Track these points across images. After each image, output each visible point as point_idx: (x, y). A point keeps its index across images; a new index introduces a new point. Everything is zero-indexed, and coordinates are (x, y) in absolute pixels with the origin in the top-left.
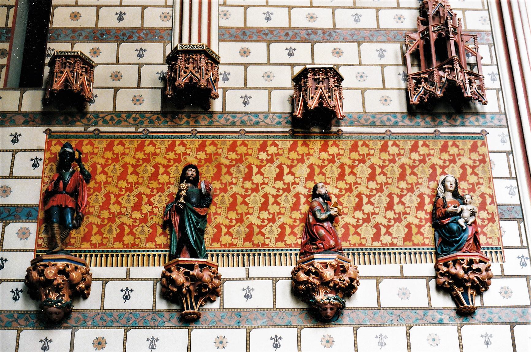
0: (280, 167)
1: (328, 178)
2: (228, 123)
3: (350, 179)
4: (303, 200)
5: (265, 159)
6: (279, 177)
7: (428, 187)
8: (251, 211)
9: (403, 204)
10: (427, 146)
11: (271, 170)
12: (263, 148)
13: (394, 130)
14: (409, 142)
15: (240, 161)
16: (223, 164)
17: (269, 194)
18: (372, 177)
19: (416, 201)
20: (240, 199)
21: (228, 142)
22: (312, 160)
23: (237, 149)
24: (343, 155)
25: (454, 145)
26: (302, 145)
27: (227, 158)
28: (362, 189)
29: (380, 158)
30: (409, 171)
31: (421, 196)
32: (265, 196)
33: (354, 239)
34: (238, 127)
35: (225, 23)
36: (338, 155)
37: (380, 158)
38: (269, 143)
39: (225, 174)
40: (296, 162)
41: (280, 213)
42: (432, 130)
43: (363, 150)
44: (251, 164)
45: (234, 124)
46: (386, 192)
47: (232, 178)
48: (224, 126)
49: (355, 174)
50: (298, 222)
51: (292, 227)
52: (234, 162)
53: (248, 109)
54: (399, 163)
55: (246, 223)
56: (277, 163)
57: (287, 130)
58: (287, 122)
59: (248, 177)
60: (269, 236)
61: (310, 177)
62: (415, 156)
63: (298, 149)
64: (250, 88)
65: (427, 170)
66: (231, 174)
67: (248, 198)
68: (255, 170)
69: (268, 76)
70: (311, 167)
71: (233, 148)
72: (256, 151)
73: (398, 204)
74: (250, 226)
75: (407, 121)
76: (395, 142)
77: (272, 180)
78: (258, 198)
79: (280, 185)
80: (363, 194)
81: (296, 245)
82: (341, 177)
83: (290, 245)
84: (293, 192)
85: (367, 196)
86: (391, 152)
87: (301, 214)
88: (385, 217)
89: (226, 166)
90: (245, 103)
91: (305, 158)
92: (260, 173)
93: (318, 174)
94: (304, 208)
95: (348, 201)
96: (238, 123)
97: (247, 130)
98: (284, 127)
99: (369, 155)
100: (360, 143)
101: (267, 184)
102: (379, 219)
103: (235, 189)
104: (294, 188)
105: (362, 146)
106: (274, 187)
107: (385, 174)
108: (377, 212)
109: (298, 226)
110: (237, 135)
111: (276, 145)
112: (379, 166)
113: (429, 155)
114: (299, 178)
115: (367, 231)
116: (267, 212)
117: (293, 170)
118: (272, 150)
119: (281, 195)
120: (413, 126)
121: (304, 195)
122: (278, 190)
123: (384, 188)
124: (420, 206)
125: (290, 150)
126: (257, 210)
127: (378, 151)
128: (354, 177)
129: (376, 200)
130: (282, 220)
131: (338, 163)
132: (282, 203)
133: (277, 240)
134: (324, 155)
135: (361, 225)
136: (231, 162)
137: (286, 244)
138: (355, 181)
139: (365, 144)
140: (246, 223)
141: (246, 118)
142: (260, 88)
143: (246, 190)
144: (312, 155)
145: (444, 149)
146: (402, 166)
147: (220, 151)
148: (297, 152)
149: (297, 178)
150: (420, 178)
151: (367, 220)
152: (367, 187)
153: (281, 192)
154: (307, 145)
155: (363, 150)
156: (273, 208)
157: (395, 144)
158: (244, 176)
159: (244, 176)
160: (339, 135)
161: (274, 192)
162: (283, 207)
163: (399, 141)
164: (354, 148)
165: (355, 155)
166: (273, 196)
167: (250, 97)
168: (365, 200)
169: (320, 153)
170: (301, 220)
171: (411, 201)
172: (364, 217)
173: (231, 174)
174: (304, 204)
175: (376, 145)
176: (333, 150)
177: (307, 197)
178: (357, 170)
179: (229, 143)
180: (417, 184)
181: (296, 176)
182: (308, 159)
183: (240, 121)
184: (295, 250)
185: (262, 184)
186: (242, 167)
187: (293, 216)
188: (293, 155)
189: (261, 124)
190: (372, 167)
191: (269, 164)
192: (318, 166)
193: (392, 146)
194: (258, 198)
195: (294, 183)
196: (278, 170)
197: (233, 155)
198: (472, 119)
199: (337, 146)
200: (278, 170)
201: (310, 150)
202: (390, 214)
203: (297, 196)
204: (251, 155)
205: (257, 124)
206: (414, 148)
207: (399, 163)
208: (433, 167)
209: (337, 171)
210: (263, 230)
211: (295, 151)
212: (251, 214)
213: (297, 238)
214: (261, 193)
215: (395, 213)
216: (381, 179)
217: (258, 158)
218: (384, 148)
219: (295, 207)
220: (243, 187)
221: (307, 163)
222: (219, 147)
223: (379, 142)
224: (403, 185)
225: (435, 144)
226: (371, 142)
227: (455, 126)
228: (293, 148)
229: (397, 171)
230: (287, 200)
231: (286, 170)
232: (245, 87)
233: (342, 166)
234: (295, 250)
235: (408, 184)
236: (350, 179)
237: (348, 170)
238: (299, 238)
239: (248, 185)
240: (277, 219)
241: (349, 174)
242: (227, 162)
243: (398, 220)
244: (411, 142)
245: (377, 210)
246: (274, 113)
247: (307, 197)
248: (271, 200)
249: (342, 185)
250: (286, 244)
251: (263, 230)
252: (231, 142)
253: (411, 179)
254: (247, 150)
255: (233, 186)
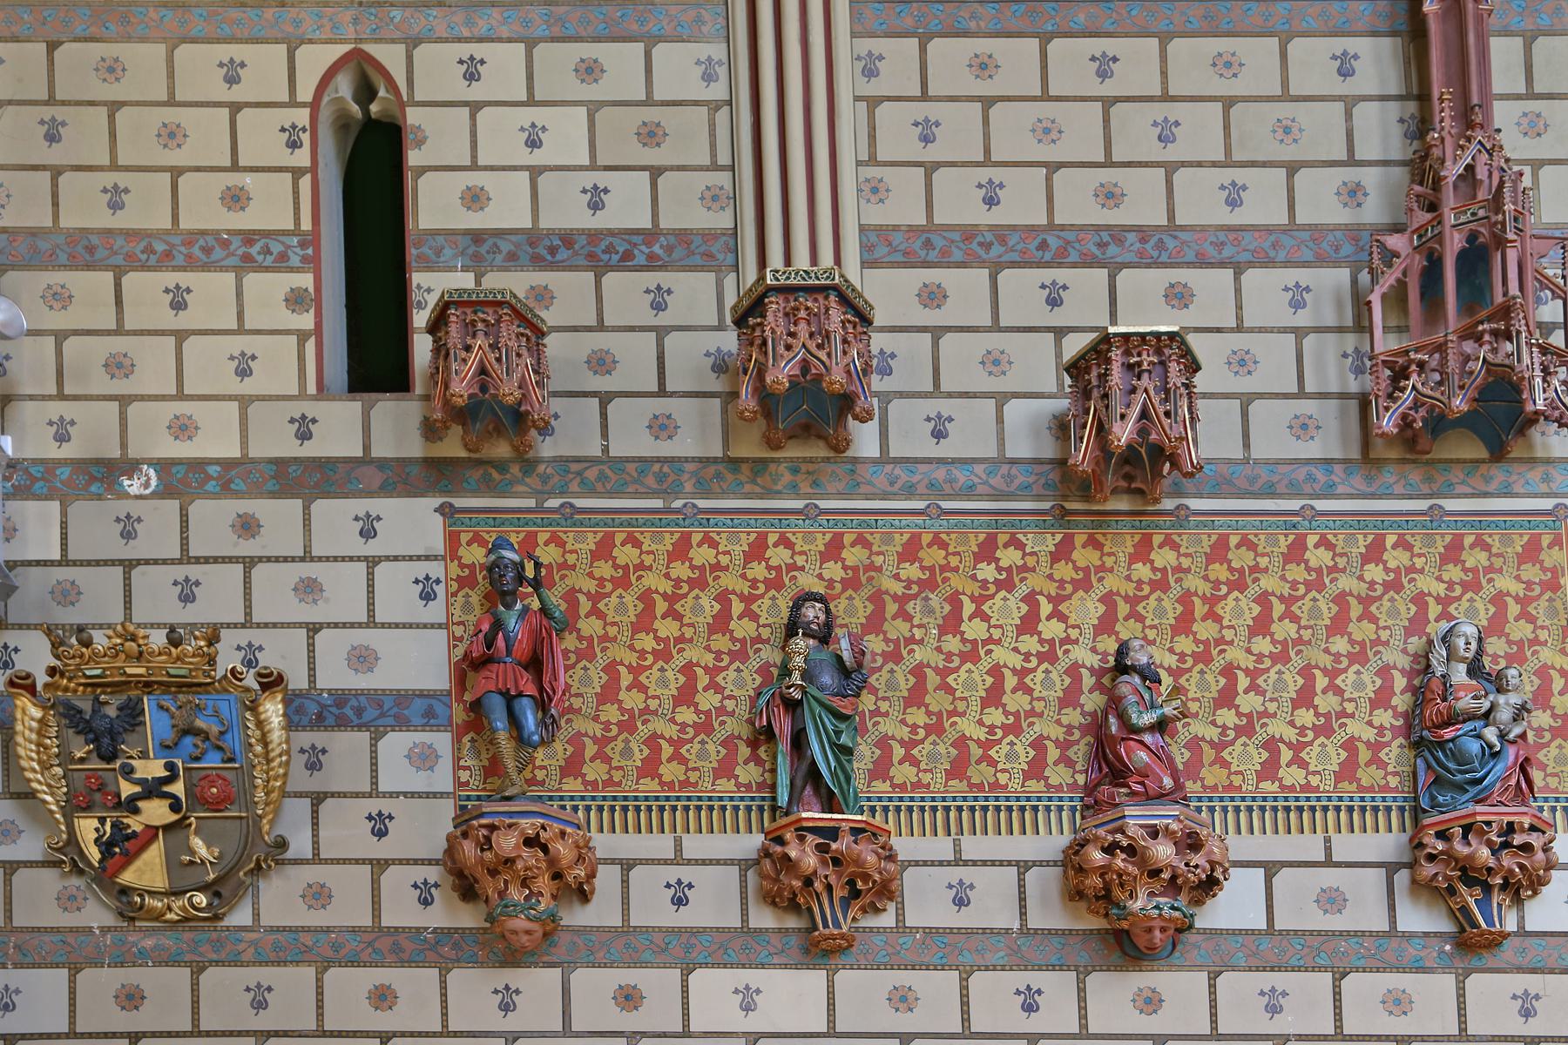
0: (1030, 599)
1: (1152, 627)
2: (897, 486)
3: (1205, 630)
4: (1088, 681)
5: (991, 580)
6: (1029, 624)
7: (1405, 651)
8: (961, 706)
9: (1339, 692)
10: (1408, 547)
11: (1008, 609)
12: (986, 552)
13: (1321, 505)
14: (1360, 537)
15: (929, 584)
16: (887, 592)
17: (1005, 666)
18: (1261, 626)
19: (1371, 683)
20: (932, 679)
21: (897, 536)
22: (1111, 583)
23: (921, 554)
24: (1188, 570)
25: (1480, 544)
26: (1084, 546)
27: (897, 577)
28: (1235, 654)
29: (1283, 578)
30: (1356, 610)
31: (1385, 672)
32: (996, 671)
33: (1212, 775)
34: (921, 497)
35: (877, 215)
36: (1178, 569)
37: (1283, 578)
38: (1002, 539)
39: (894, 618)
40: (1069, 588)
41: (1032, 713)
42: (1422, 505)
43: (1241, 558)
44: (957, 593)
45: (909, 492)
46: (1297, 662)
47: (913, 626)
48: (885, 496)
49: (1218, 619)
50: (1077, 734)
51: (1064, 746)
52: (915, 588)
53: (945, 450)
54: (1332, 589)
55: (951, 735)
56: (1022, 590)
57: (1047, 505)
58: (1046, 485)
59: (952, 624)
60: (1008, 766)
61: (1106, 625)
62: (1374, 572)
63: (1075, 555)
64: (950, 395)
65: (1403, 609)
66: (908, 618)
67: (954, 676)
68: (968, 607)
69: (996, 362)
70: (1108, 599)
71: (910, 553)
72: (969, 560)
73: (1324, 691)
74: (961, 742)
75: (1358, 482)
76: (1323, 536)
77: (1011, 632)
78: (976, 676)
79: (1030, 643)
80: (1239, 668)
81: (1074, 786)
82: (1184, 624)
83: (1059, 788)
84: (1064, 663)
85: (1247, 671)
86: (1313, 564)
87: (1083, 714)
88: (1292, 723)
89: (895, 598)
90: (939, 435)
91: (1094, 579)
92: (979, 614)
93: (1126, 619)
94: (1092, 701)
95: (1202, 685)
96: (921, 489)
97: (945, 505)
98: (1039, 498)
99: (1255, 569)
100: (1234, 540)
101: (998, 642)
102: (1278, 728)
103: (920, 654)
104: (1067, 652)
105: (1238, 546)
106: (1016, 650)
107: (1295, 619)
108: (1271, 711)
109: (1077, 742)
110: (919, 520)
111: (1020, 546)
112: (1281, 598)
113: (1411, 569)
114: (1078, 627)
115: (1246, 757)
116: (1001, 710)
117: (1062, 608)
118: (1009, 557)
119: (1034, 670)
120: (1373, 496)
121: (1092, 670)
122: (1027, 657)
123: (1292, 654)
124: (1381, 699)
125: (1055, 557)
126: (975, 706)
127: (1278, 561)
128: (1216, 627)
129: (1270, 682)
130: (1037, 728)
131: (1176, 591)
132: (1038, 688)
133: (1027, 776)
134: (1142, 571)
135: (1232, 743)
136: (908, 587)
137: (1048, 786)
138: (1217, 636)
139: (1245, 543)
140: (951, 735)
141: (940, 474)
142: (974, 395)
143: (949, 657)
144: (1111, 570)
145: (1453, 553)
146: (1341, 599)
147: (878, 560)
148: (1074, 563)
149: (1074, 627)
150: (1385, 628)
151: (1246, 730)
152: (1249, 651)
153: (1034, 662)
154: (1098, 546)
155: (1241, 558)
156: (1016, 702)
157: (1324, 542)
158: (940, 622)
159: (940, 622)
160: (1181, 517)
161: (1016, 661)
162: (1039, 699)
163: (1335, 535)
164: (1219, 551)
165: (1219, 571)
166: (1014, 670)
167: (950, 419)
168: (1243, 682)
169: (1130, 564)
170: (1085, 730)
171: (1359, 686)
172: (1238, 722)
173: (908, 618)
174: (1091, 692)
175: (1276, 543)
176: (1164, 558)
177: (1098, 673)
178: (1226, 609)
179: (900, 540)
180: (1377, 642)
181: (1071, 622)
182: (1100, 580)
183: (926, 481)
184: (1071, 799)
185: (985, 642)
186: (935, 600)
187: (1065, 720)
188: (1064, 571)
189: (981, 489)
190: (1263, 599)
191: (1003, 593)
192: (1127, 599)
193: (1317, 546)
194: (976, 676)
195: (1067, 640)
196: (1025, 608)
197: (911, 571)
198: (1534, 475)
199: (1175, 547)
200: (1025, 608)
201: (1105, 558)
202: (1306, 717)
203: (1074, 670)
204: (956, 570)
205: (969, 493)
206: (1374, 553)
207: (1332, 589)
208: (1420, 600)
209: (1172, 610)
210: (992, 753)
211: (1069, 559)
212: (963, 714)
213: (1075, 772)
214: (986, 663)
215: (1317, 715)
216: (1284, 629)
217: (974, 577)
218: (1296, 552)
219: (1070, 698)
220: (939, 649)
221: (1099, 590)
222: (875, 548)
223: (1282, 538)
224: (1340, 645)
225: (1429, 541)
226: (1262, 537)
227: (1486, 495)
228: (1062, 553)
229: (1327, 610)
230: (1049, 683)
231: (1046, 608)
232: (937, 392)
233: (1186, 599)
234: (1071, 799)
235: (1352, 642)
236: (1205, 630)
237: (1200, 609)
238: (1080, 772)
239: (952, 644)
240: (1024, 725)
241: (1204, 619)
242: (897, 588)
243: (1325, 730)
244: (1365, 535)
245: (1272, 707)
246: (1013, 462)
247: (1098, 673)
248: (1011, 681)
249: (1185, 644)
250: (1048, 786)
251: (992, 753)
252: (906, 537)
253: (1363, 631)
254: (945, 558)
255: (915, 647)
